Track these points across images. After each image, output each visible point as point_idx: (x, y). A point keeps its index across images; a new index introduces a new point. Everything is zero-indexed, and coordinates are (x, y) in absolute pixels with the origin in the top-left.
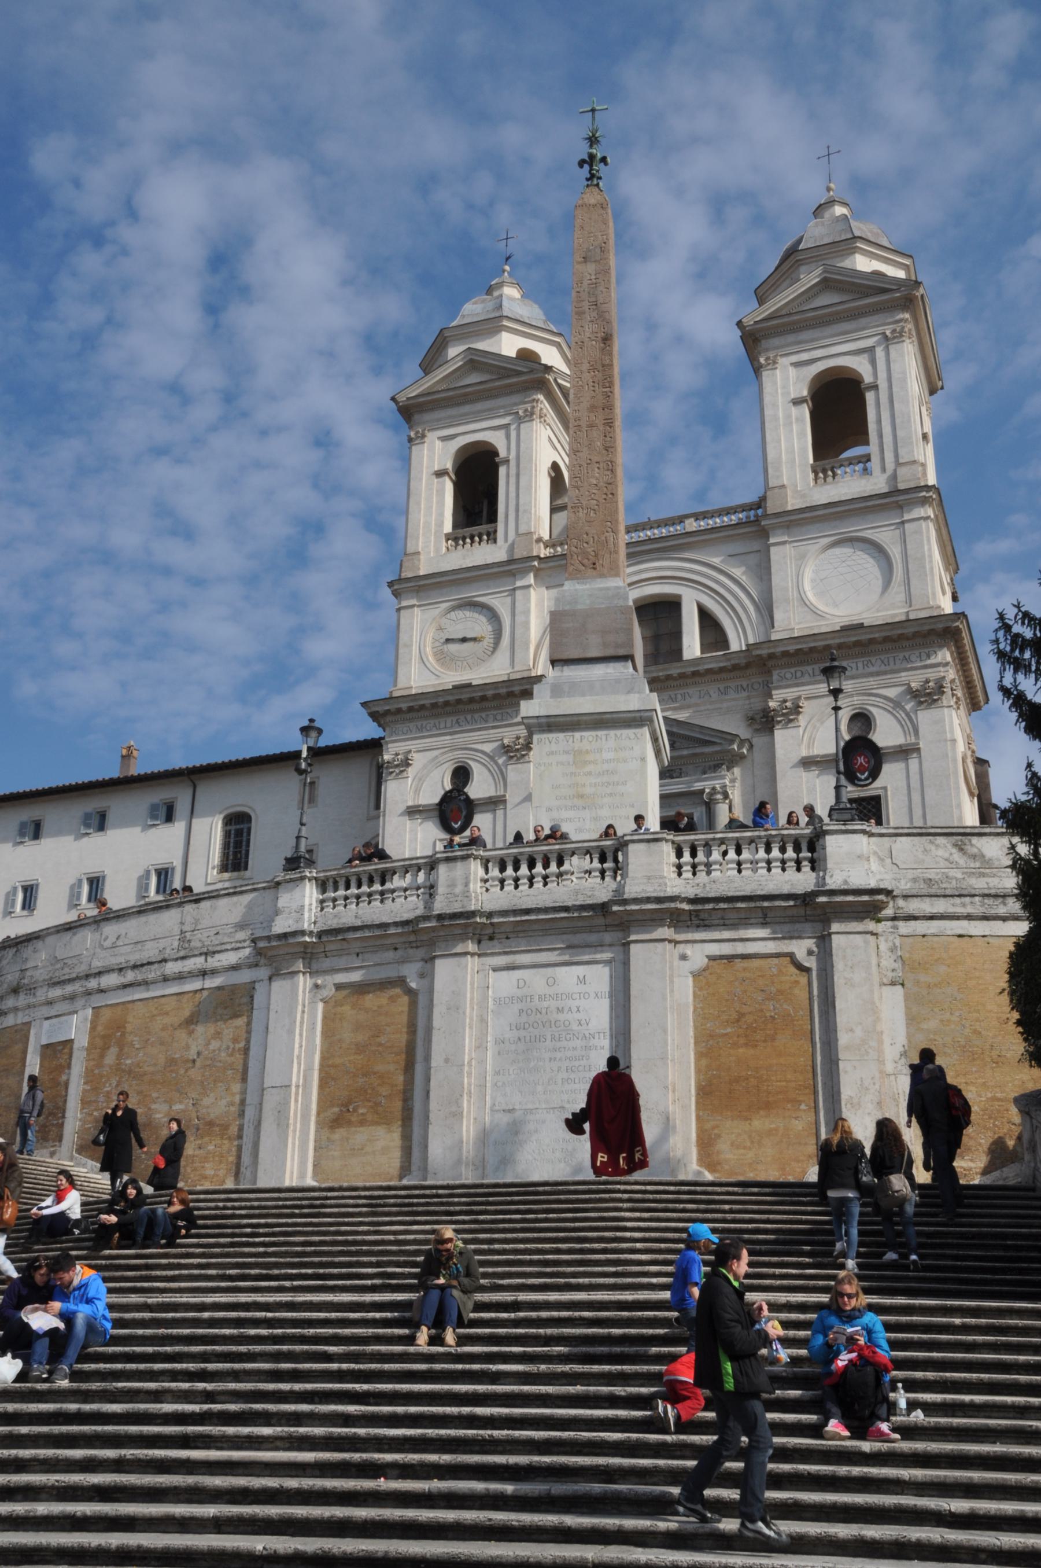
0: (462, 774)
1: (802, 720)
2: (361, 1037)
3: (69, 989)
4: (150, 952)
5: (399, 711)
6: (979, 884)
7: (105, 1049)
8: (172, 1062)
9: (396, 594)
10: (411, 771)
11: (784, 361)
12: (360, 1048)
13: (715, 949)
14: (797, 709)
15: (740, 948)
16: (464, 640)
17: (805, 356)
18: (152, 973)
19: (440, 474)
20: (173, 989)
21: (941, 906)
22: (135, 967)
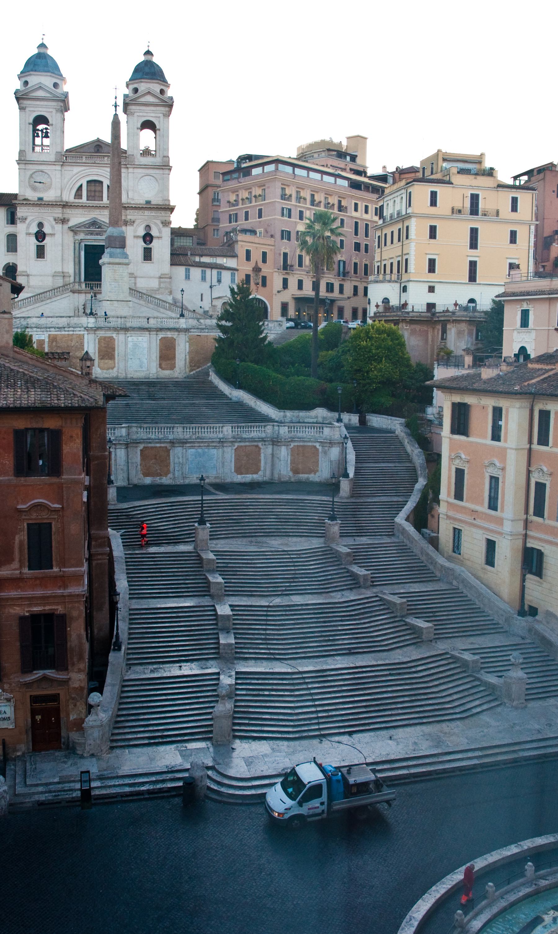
0: (40, 225)
1: (135, 225)
2: (106, 345)
3: (42, 330)
4: (60, 326)
5: (23, 204)
6: (200, 327)
7: (52, 343)
8: (68, 346)
9: (18, 164)
10: (27, 222)
11: (136, 114)
12: (105, 347)
13: (163, 336)
14: (134, 222)
15: (166, 336)
16: (40, 183)
17: (141, 114)
18: (63, 329)
19: (30, 124)
20: (67, 333)
21: (195, 330)
22: (58, 328)
